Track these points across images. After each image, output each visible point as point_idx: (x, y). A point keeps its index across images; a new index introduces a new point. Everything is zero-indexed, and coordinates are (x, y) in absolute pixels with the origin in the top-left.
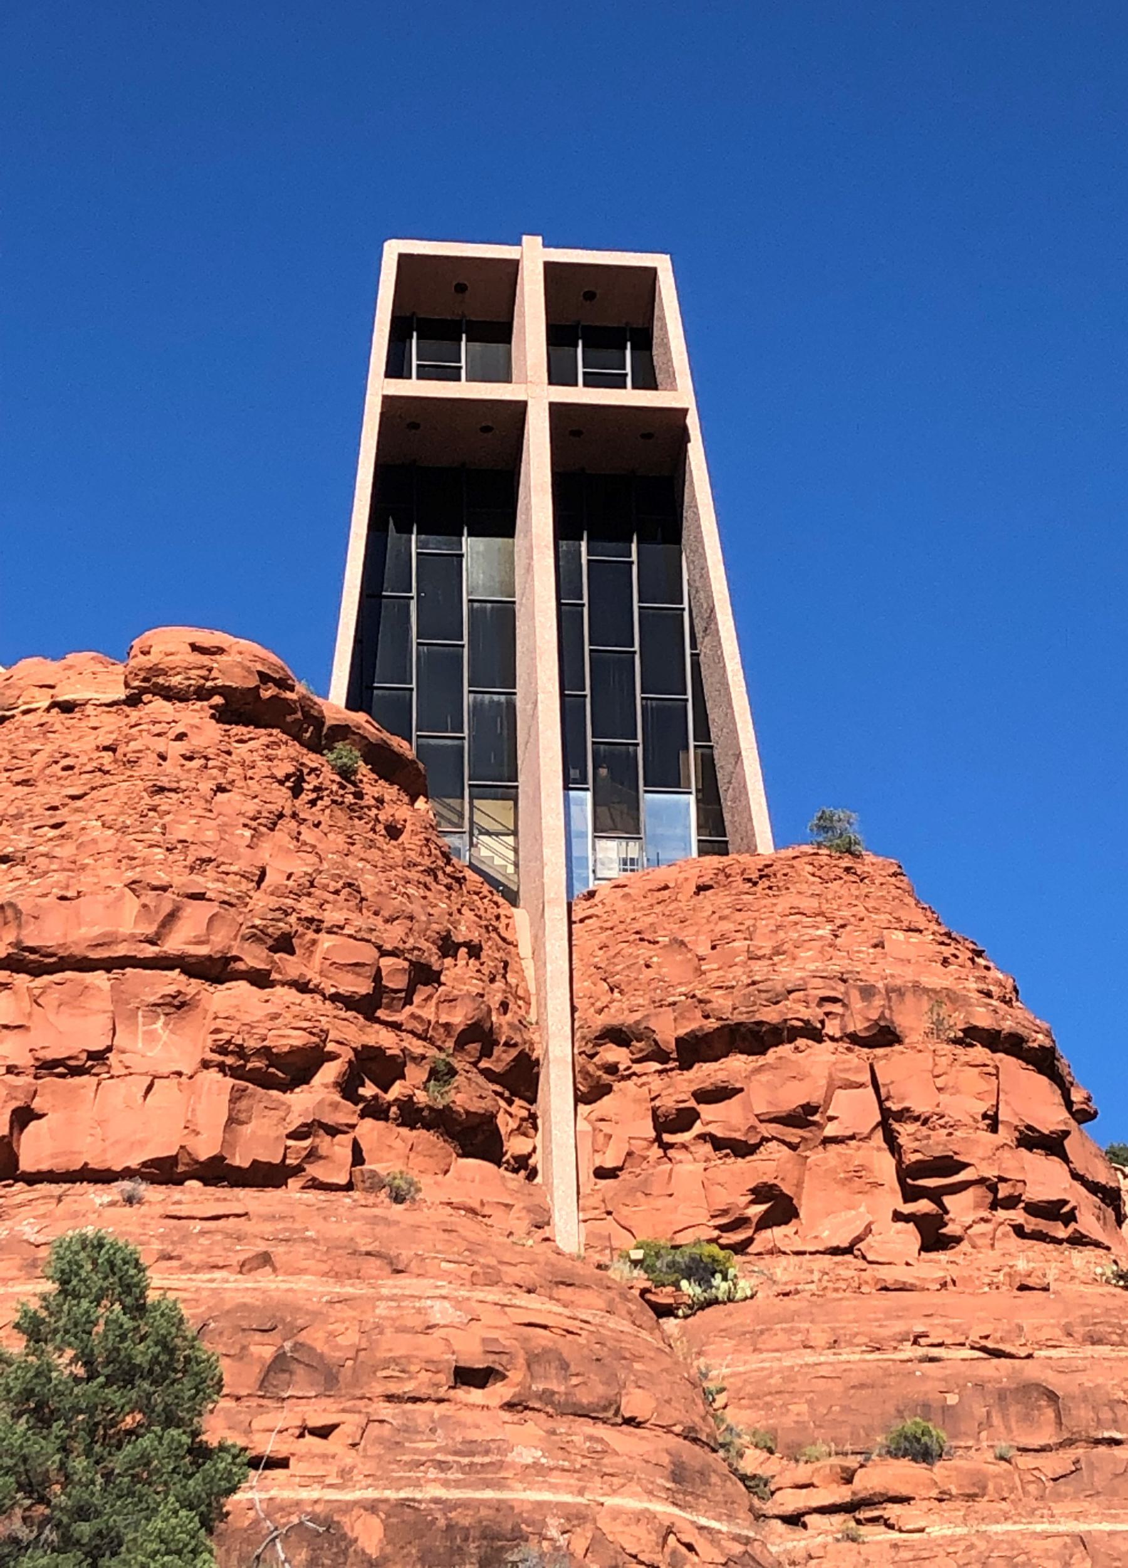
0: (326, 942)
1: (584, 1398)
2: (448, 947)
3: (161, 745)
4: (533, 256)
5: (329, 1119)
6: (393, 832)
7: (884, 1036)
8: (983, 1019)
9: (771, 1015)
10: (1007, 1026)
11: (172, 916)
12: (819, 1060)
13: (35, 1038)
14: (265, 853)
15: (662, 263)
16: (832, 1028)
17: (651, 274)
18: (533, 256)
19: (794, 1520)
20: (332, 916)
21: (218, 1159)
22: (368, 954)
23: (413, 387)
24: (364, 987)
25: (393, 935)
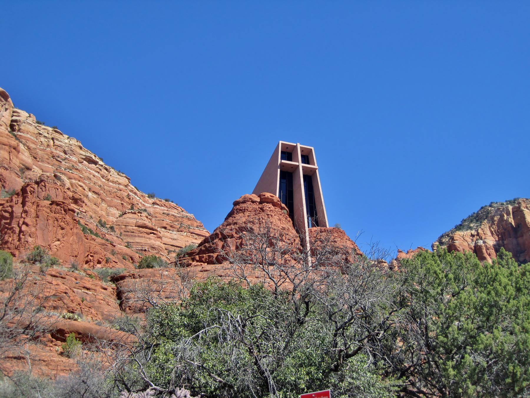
18: (299, 146)
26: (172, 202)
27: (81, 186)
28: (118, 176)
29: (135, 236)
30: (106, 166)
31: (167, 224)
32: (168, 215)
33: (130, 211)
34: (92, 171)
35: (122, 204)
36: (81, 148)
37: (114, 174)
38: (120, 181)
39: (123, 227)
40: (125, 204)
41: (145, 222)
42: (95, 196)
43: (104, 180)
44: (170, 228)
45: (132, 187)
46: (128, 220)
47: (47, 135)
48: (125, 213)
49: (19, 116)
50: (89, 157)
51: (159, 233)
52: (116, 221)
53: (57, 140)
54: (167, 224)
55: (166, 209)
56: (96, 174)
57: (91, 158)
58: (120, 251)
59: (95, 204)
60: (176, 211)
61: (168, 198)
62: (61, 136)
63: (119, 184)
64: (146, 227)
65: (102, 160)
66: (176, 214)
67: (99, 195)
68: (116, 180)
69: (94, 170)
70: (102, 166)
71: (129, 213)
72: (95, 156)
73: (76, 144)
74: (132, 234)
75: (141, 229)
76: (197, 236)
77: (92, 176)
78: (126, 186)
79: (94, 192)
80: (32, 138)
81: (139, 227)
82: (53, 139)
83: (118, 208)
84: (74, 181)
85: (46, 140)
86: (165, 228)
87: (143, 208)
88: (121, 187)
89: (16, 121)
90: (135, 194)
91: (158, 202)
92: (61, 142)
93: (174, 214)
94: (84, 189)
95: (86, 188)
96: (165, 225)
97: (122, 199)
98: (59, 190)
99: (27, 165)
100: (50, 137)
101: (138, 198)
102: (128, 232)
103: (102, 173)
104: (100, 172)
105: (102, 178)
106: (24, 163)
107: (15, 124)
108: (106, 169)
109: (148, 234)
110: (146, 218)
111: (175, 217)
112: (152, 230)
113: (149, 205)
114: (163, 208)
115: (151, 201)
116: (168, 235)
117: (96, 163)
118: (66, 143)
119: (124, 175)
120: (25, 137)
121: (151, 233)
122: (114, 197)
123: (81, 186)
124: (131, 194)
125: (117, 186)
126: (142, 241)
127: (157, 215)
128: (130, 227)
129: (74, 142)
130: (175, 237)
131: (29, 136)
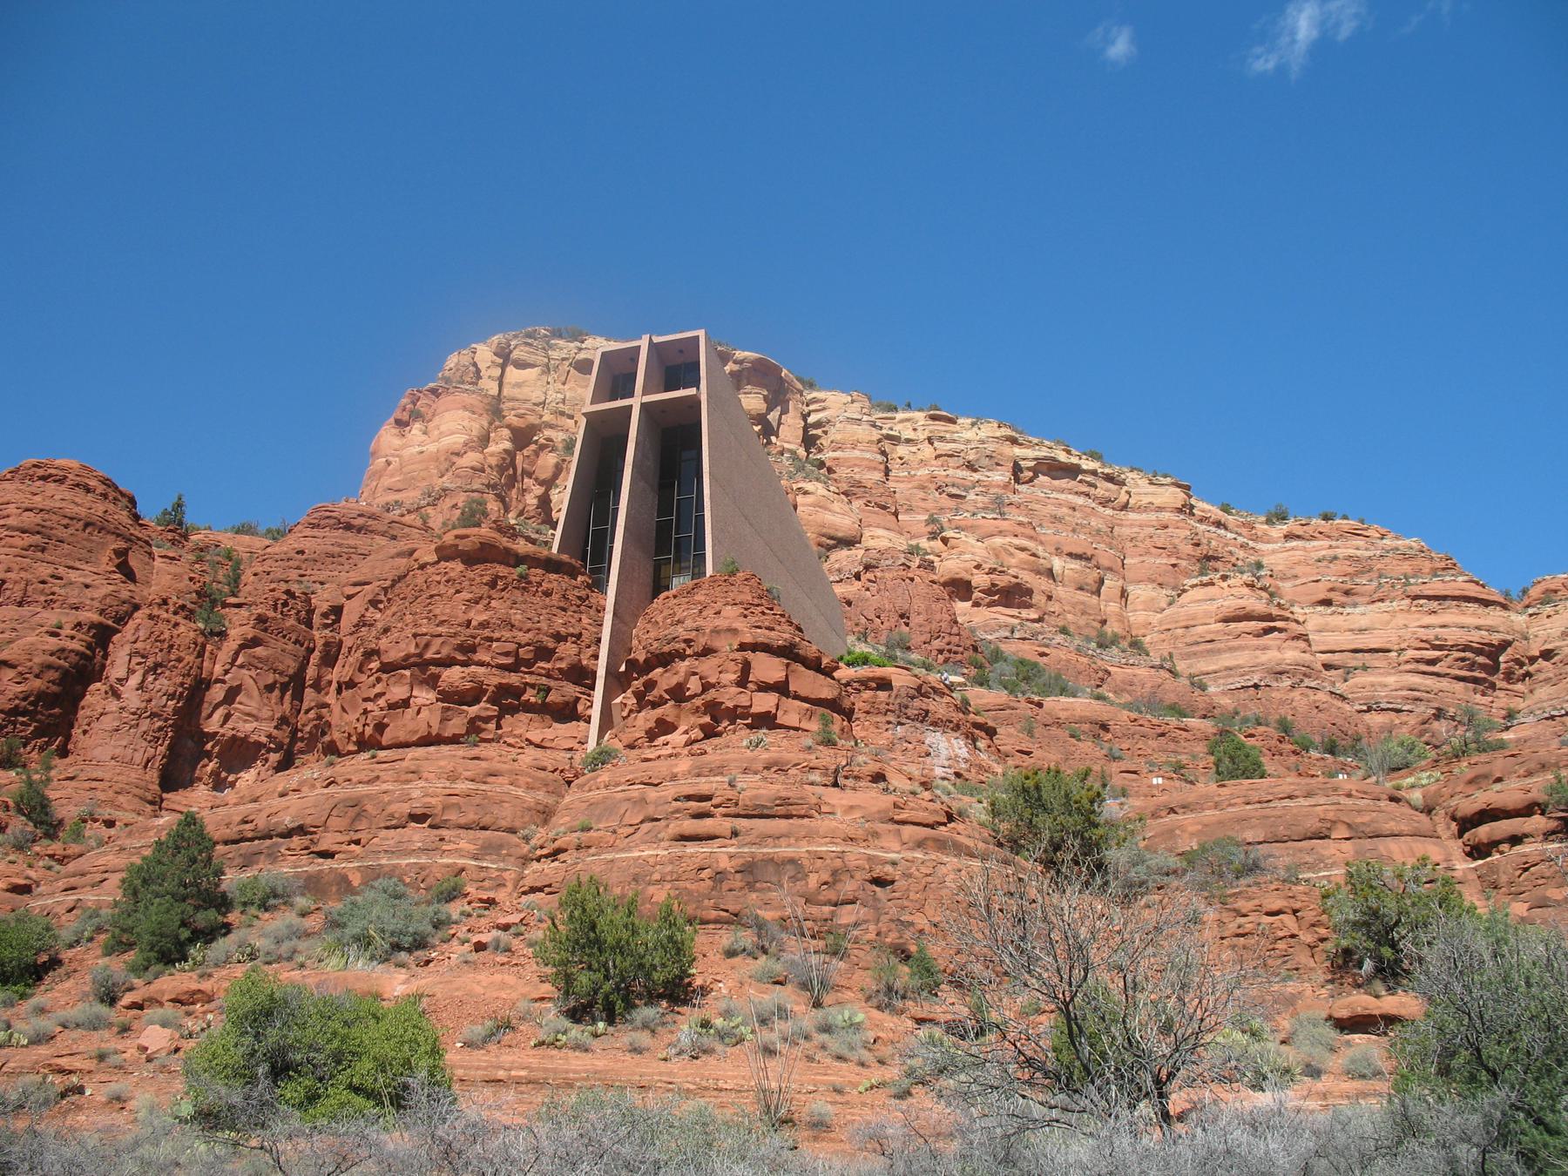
0: (495, 644)
1: (462, 821)
2: (559, 638)
3: (438, 578)
4: (644, 343)
5: (484, 714)
6: (548, 594)
7: (707, 651)
8: (748, 639)
9: (666, 649)
10: (760, 640)
11: (427, 645)
12: (682, 666)
13: (387, 696)
14: (471, 615)
15: (701, 333)
16: (689, 652)
17: (697, 338)
19: (538, 860)
20: (496, 635)
21: (438, 735)
22: (511, 647)
23: (692, 391)
24: (510, 660)
25: (523, 638)
26: (1345, 517)
27: (1023, 549)
28: (1152, 489)
29: (1219, 651)
30: (1107, 471)
31: (1332, 590)
32: (1335, 558)
33: (1195, 581)
34: (1063, 496)
35: (1174, 566)
36: (1014, 441)
37: (1139, 487)
38: (1158, 501)
39: (1180, 631)
40: (1183, 563)
41: (1242, 603)
42: (1076, 565)
43: (1109, 512)
44: (1344, 599)
45: (1201, 506)
46: (1194, 609)
47: (911, 435)
48: (1184, 591)
49: (824, 409)
50: (1045, 458)
51: (1293, 625)
52: (1161, 623)
53: (942, 439)
54: (1332, 590)
55: (1326, 543)
56: (1080, 500)
57: (1054, 459)
58: (1063, 715)
59: (1081, 589)
60: (1360, 542)
61: (1329, 510)
62: (951, 427)
63: (1160, 509)
64: (1248, 617)
65: (1094, 456)
66: (1359, 553)
67: (1088, 559)
68: (1145, 500)
69: (1070, 491)
70: (1094, 473)
71: (1193, 586)
72: (1069, 452)
73: (998, 434)
74: (1209, 646)
75: (1233, 625)
76: (1434, 605)
77: (1065, 510)
78: (1180, 511)
79: (1070, 555)
80: (868, 455)
81: (1226, 620)
82: (930, 440)
83: (1160, 580)
84: (998, 541)
85: (914, 449)
86: (1327, 603)
87: (1252, 559)
88: (1166, 516)
89: (818, 425)
90: (1218, 524)
91: (1299, 531)
92: (954, 441)
93: (1352, 552)
94: (1034, 555)
95: (1040, 550)
96: (1322, 596)
97: (1175, 552)
98: (917, 579)
99: (840, 535)
100: (922, 437)
101: (1230, 535)
102: (1198, 643)
103: (1100, 492)
104: (1092, 491)
105: (1101, 509)
106: (832, 532)
107: (819, 432)
108: (1109, 478)
109: (1258, 636)
110: (1246, 590)
111: (1358, 559)
112: (1269, 624)
113: (1270, 546)
114: (1315, 543)
115: (1279, 530)
116: (1337, 620)
117: (1072, 471)
118: (968, 441)
119: (1169, 480)
120: (846, 460)
121: (1268, 631)
122: (1148, 553)
123: (1023, 549)
124: (1202, 527)
125: (1152, 516)
126: (1241, 662)
127: (1299, 570)
128: (1200, 629)
129: (989, 430)
130: (1364, 622)
131: (857, 453)
